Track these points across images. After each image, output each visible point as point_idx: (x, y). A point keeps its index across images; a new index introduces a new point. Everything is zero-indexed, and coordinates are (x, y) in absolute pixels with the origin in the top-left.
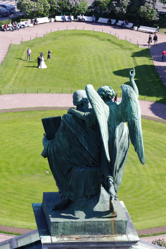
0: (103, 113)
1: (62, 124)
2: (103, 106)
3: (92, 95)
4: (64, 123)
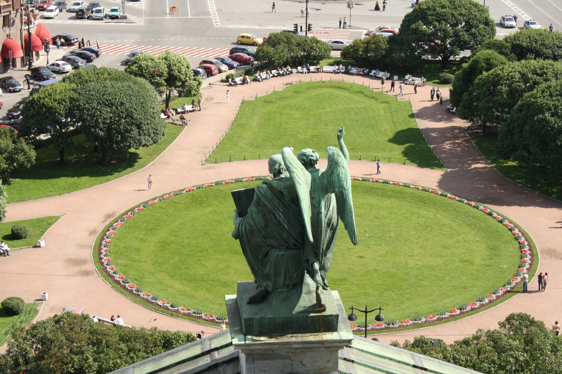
0: (303, 182)
1: (255, 197)
2: (304, 173)
3: (290, 160)
4: (257, 195)
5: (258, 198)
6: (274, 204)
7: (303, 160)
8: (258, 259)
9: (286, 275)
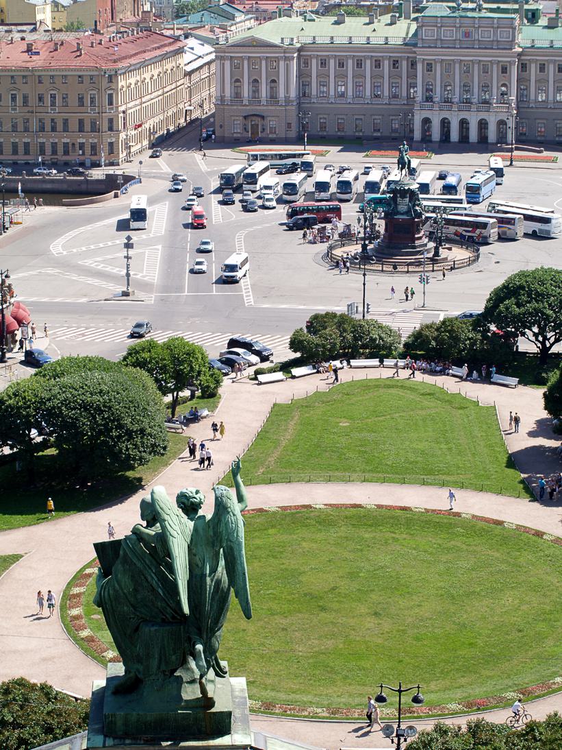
1: (121, 552)
5: (125, 554)
6: (145, 561)
7: (183, 503)
8: (125, 634)
9: (161, 657)
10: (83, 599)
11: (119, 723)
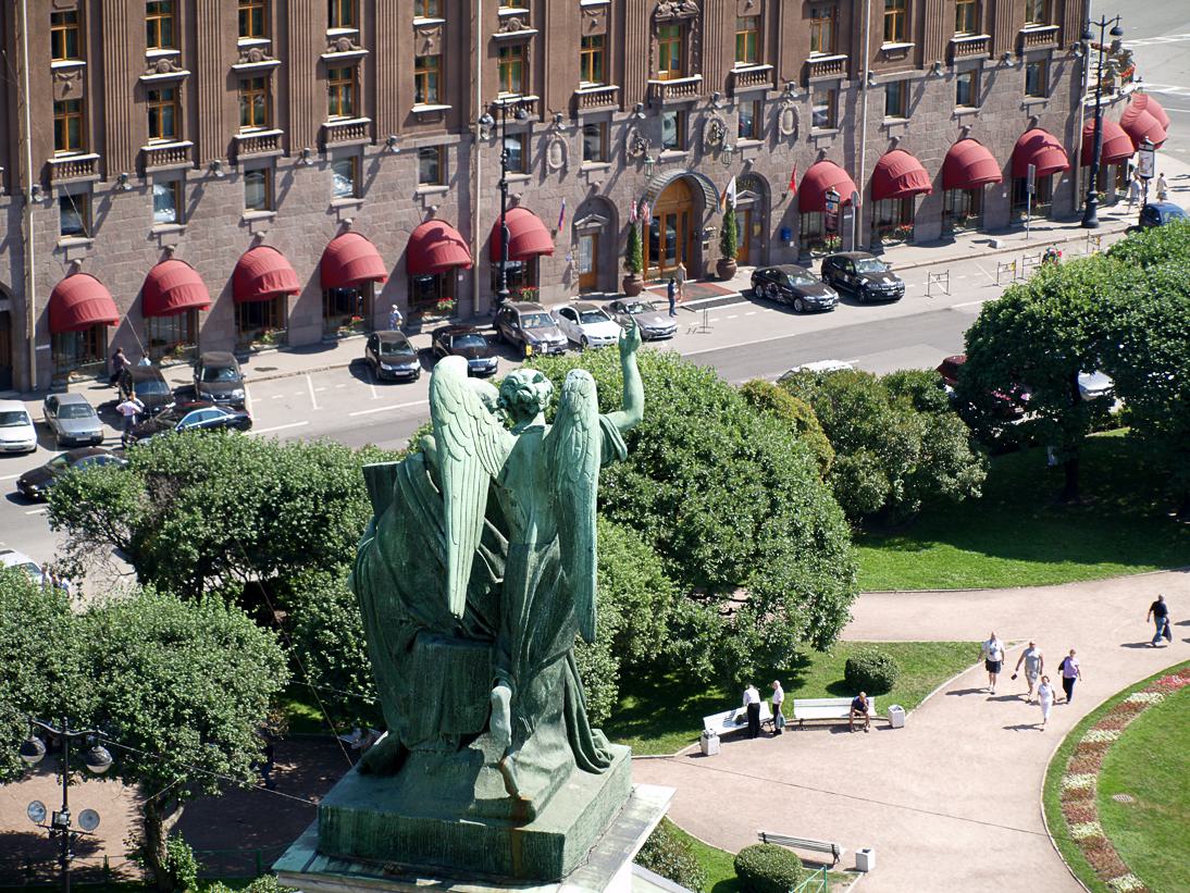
6: (428, 507)
8: (391, 655)
9: (441, 712)
10: (1107, 757)
11: (347, 829)
